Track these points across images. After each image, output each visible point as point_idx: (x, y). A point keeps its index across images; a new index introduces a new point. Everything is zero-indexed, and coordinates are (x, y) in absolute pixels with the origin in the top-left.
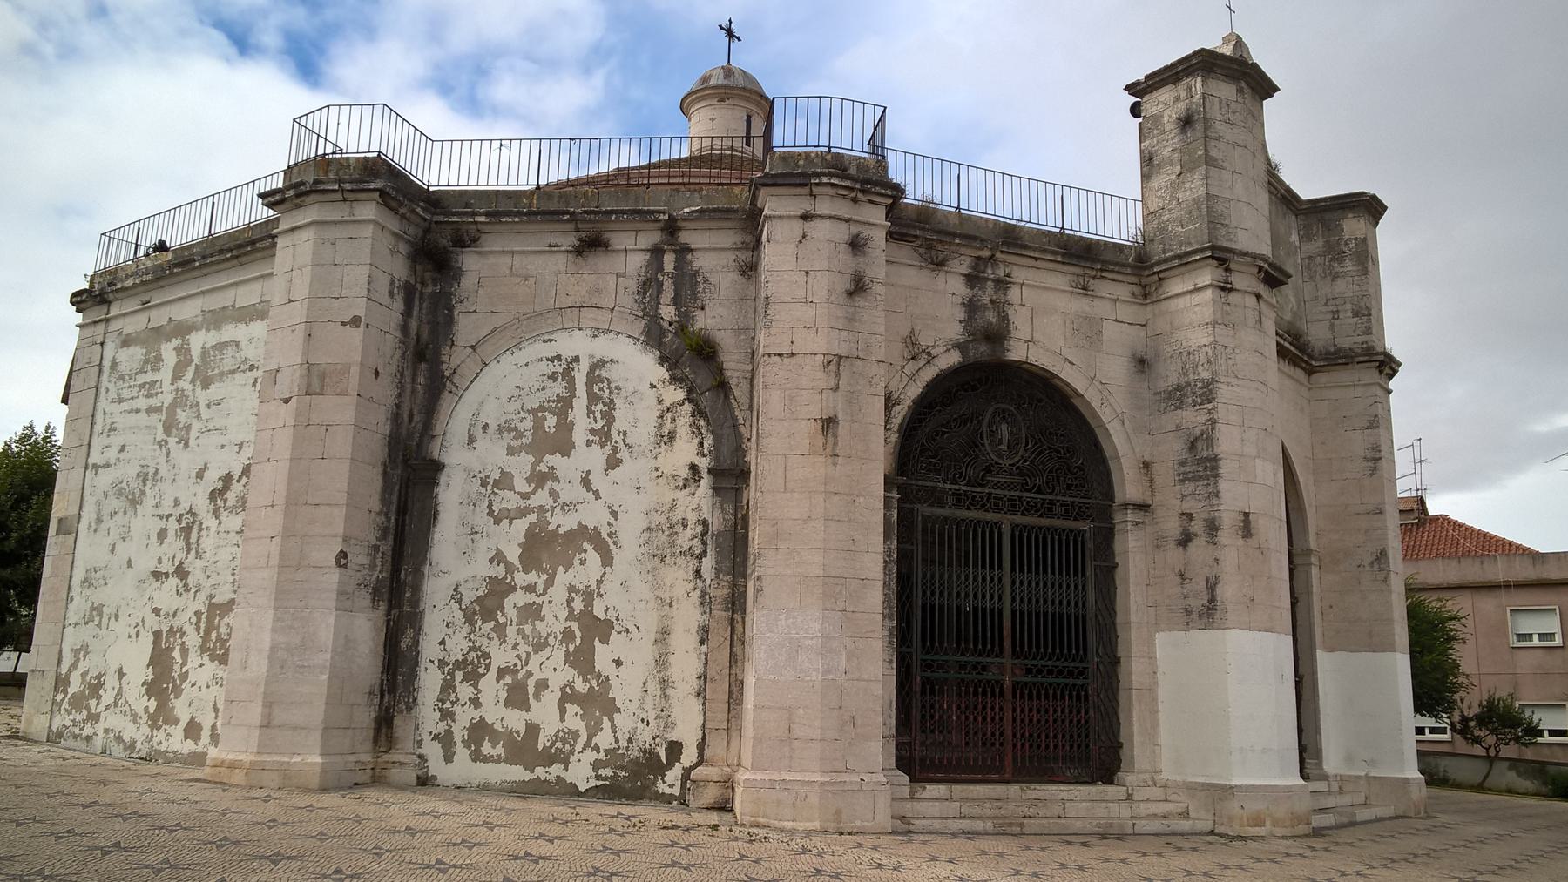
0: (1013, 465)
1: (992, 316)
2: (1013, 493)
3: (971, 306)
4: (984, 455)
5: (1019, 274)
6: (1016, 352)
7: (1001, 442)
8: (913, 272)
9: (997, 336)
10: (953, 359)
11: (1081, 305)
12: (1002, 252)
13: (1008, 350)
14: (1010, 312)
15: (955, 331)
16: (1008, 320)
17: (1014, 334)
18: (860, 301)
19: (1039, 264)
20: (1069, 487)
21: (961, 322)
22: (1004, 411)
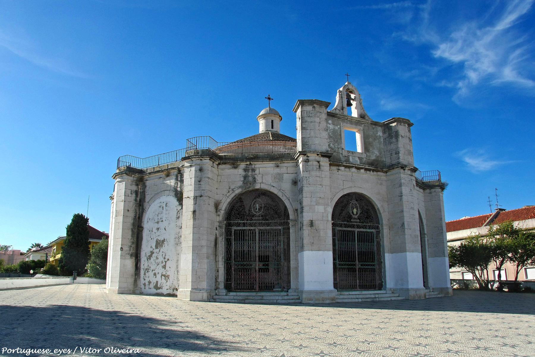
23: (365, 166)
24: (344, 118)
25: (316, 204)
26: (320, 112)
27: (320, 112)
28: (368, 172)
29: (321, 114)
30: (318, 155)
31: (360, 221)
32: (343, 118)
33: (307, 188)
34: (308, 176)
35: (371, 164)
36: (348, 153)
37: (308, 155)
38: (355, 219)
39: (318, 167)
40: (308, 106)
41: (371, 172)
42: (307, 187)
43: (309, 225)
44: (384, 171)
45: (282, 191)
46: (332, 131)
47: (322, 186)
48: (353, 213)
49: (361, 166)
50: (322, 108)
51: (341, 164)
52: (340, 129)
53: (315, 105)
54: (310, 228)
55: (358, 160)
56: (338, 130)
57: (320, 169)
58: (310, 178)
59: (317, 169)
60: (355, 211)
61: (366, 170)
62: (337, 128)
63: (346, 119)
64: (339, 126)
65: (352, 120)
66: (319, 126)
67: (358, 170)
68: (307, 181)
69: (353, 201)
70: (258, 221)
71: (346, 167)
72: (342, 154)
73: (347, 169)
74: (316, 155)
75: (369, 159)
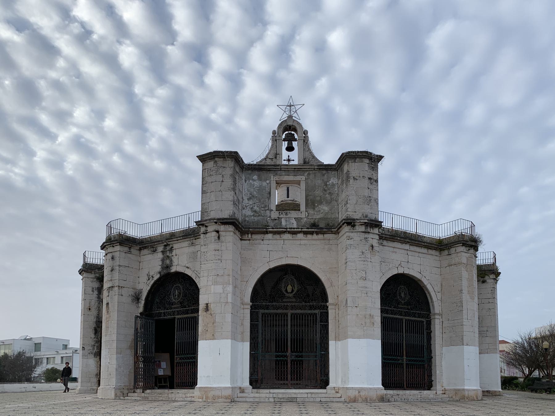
0: (179, 301)
1: (168, 262)
2: (178, 309)
3: (163, 260)
4: (171, 300)
5: (175, 246)
6: (173, 270)
7: (176, 296)
8: (150, 255)
9: (168, 267)
10: (158, 276)
11: (192, 249)
12: (169, 242)
13: (171, 270)
14: (172, 258)
15: (159, 269)
16: (172, 261)
17: (173, 264)
18: (113, 272)
19: (179, 241)
20: (193, 304)
21: (160, 265)
22: (177, 286)
23: (302, 229)
24: (276, 168)
25: (212, 283)
26: (224, 167)
27: (224, 167)
28: (309, 236)
29: (225, 169)
30: (216, 223)
31: (297, 301)
32: (274, 169)
33: (205, 265)
34: (206, 250)
35: (314, 225)
36: (280, 215)
37: (206, 225)
38: (289, 297)
39: (216, 238)
40: (210, 162)
41: (315, 235)
42: (204, 264)
43: (204, 309)
44: (334, 232)
45: (196, 272)
46: (258, 189)
47: (221, 261)
48: (286, 291)
49: (295, 230)
50: (226, 160)
51: (265, 230)
52: (269, 185)
53: (216, 159)
54: (205, 313)
55: (295, 222)
56: (267, 187)
57: (219, 239)
58: (208, 252)
59: (215, 240)
60: (289, 288)
61: (306, 233)
62: (264, 184)
63: (279, 170)
64: (268, 182)
65: (289, 169)
66: (221, 186)
67: (294, 236)
68: (205, 257)
69: (288, 276)
70: (176, 310)
71: (275, 233)
72: (270, 217)
73: (277, 236)
74: (214, 223)
75: (312, 219)
